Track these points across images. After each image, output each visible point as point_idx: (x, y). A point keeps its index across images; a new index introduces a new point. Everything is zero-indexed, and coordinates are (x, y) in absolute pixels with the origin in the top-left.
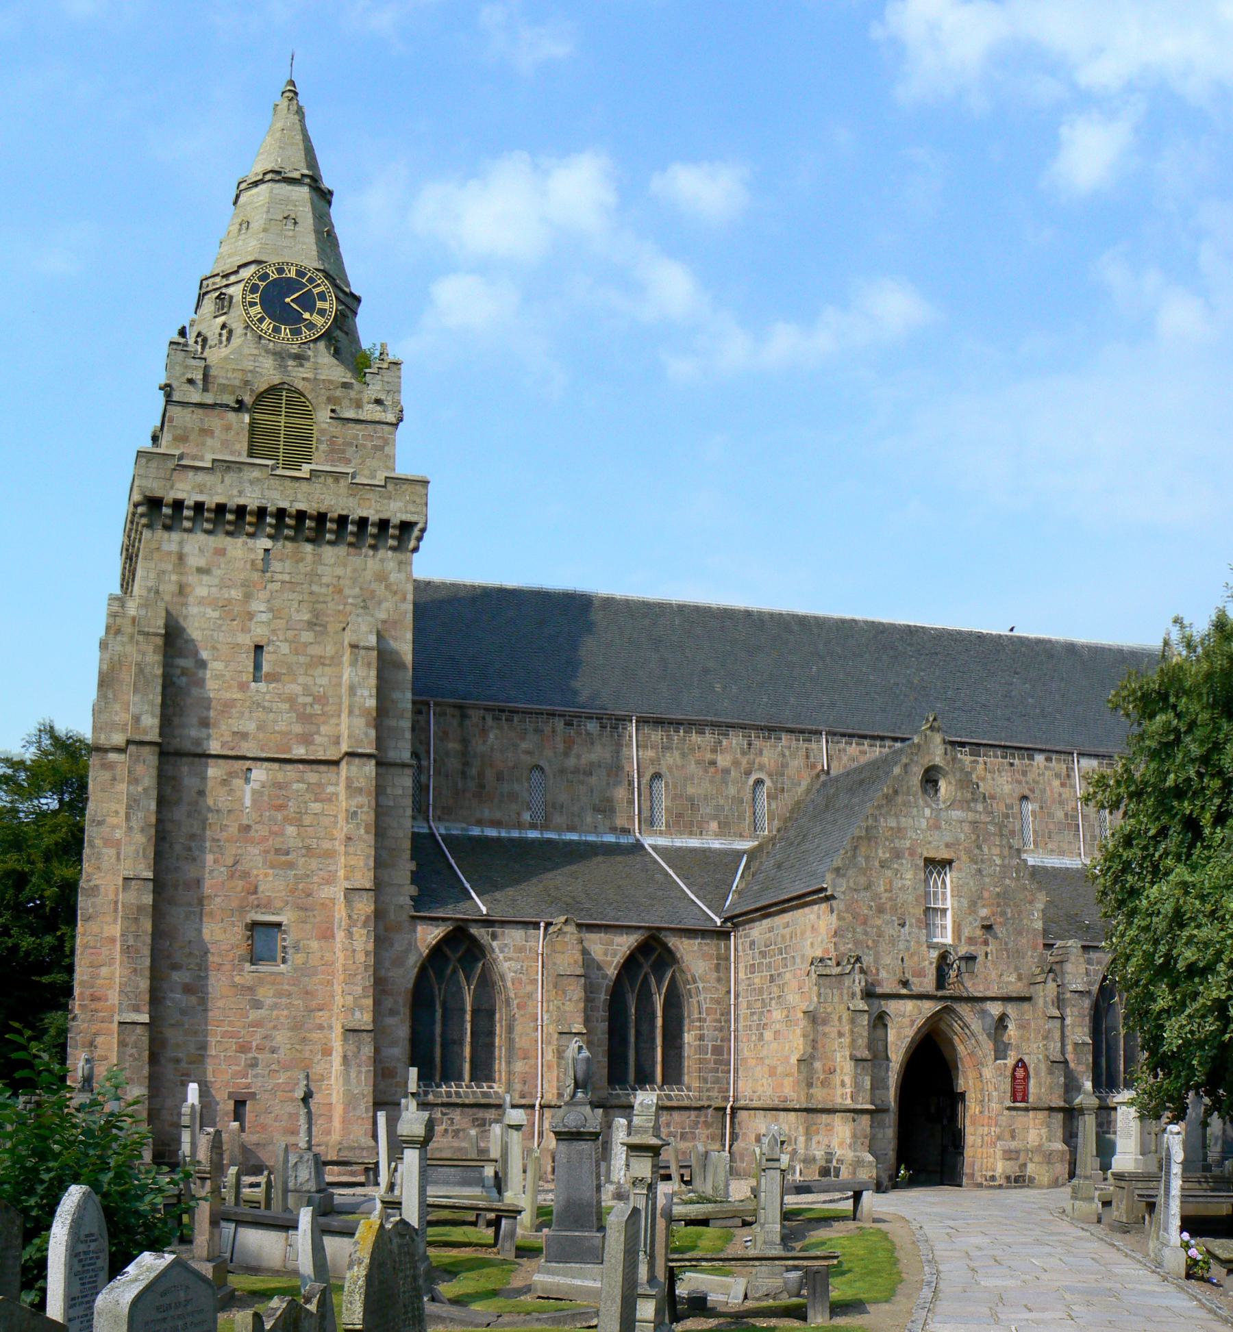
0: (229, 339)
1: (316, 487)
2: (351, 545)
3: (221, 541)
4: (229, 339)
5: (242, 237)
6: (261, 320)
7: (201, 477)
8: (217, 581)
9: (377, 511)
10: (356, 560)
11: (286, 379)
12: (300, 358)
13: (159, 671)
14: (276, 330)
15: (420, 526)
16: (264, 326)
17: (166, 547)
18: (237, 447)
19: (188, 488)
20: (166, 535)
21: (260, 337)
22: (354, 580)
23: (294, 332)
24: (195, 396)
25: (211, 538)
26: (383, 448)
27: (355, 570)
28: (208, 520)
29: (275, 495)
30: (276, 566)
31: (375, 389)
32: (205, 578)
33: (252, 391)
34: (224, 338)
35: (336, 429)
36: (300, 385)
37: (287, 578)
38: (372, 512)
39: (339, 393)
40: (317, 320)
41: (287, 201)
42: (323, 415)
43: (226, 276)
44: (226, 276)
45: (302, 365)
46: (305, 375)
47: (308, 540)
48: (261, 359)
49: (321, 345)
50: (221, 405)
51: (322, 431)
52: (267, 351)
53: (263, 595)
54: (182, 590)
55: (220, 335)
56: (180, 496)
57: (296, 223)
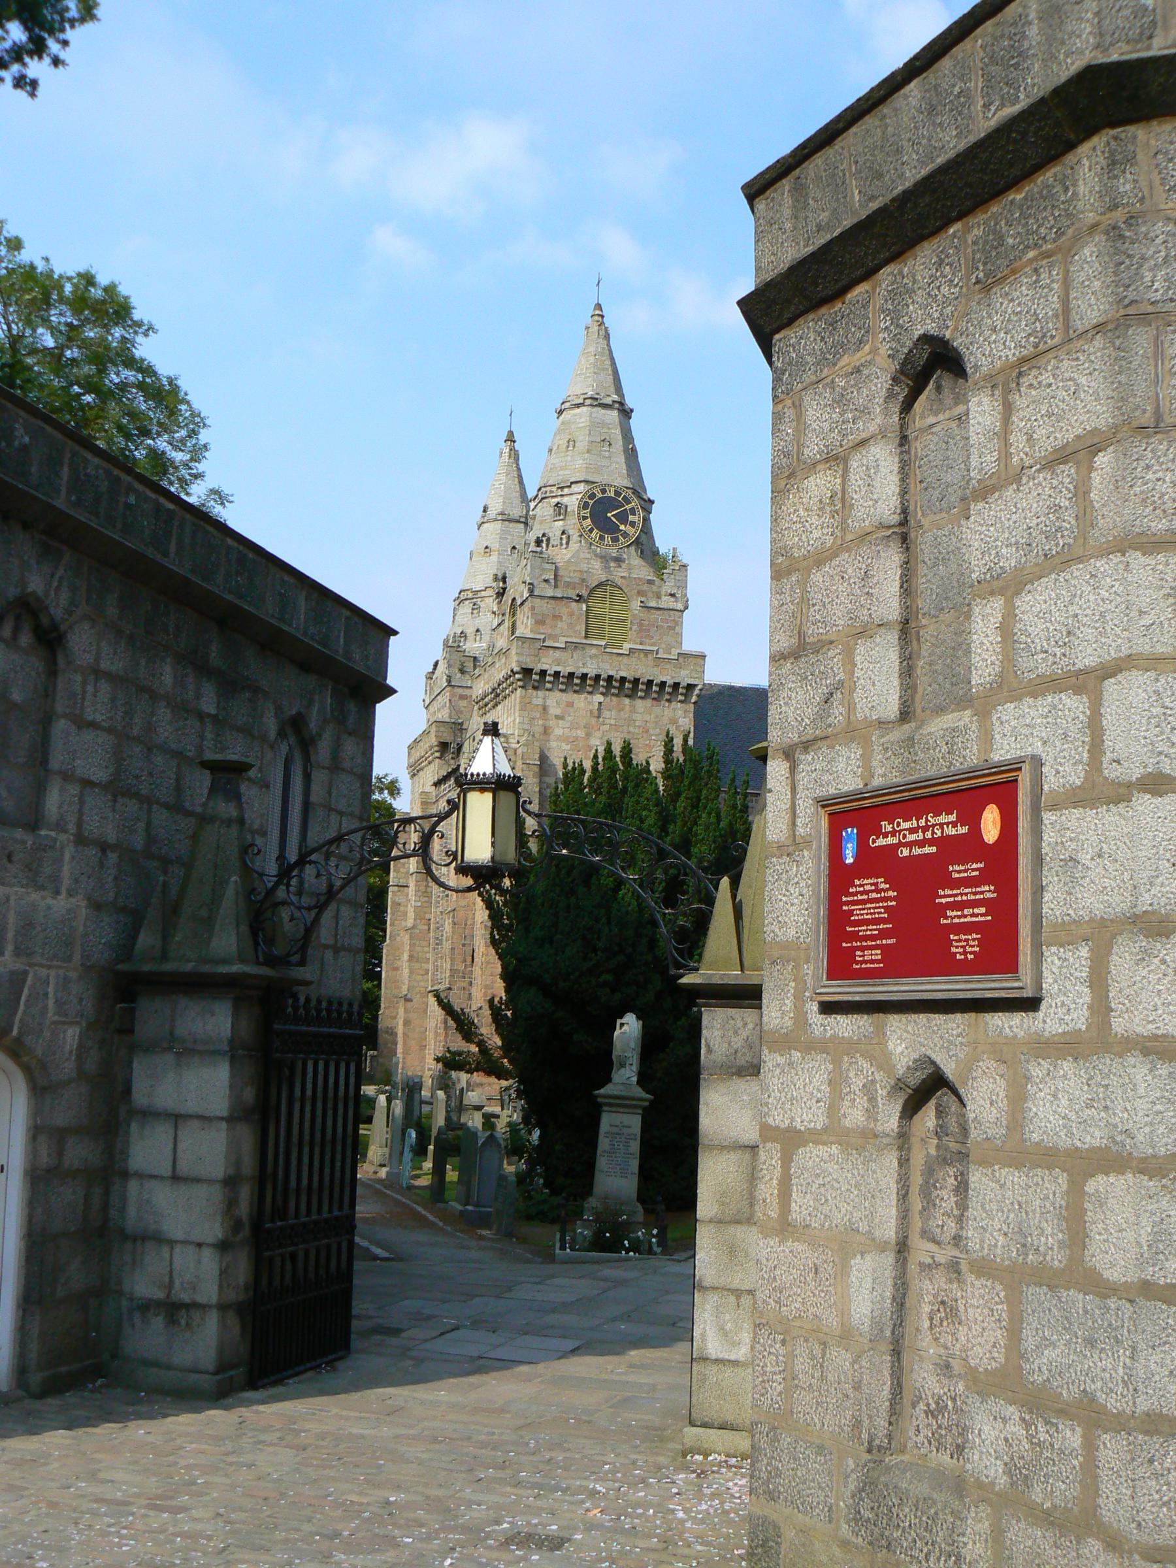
0: (567, 543)
1: (633, 660)
2: (654, 699)
3: (569, 696)
4: (567, 543)
5: (570, 453)
6: (591, 531)
7: (557, 654)
8: (568, 725)
9: (673, 678)
10: (657, 710)
11: (610, 577)
12: (618, 560)
13: (537, 789)
14: (602, 538)
15: (699, 687)
16: (593, 535)
17: (535, 701)
18: (578, 628)
19: (550, 662)
20: (535, 692)
21: (591, 544)
22: (656, 723)
23: (615, 540)
24: (550, 592)
25: (564, 695)
26: (675, 628)
27: (657, 716)
28: (562, 683)
29: (606, 666)
30: (606, 714)
31: (669, 586)
32: (561, 722)
33: (587, 586)
34: (564, 542)
35: (644, 615)
36: (619, 582)
37: (613, 722)
38: (669, 677)
39: (645, 587)
40: (630, 530)
41: (603, 424)
42: (636, 604)
43: (562, 488)
44: (562, 488)
45: (620, 567)
46: (623, 574)
47: (627, 696)
48: (592, 562)
49: (632, 549)
50: (567, 598)
51: (634, 616)
52: (596, 555)
53: (598, 734)
54: (546, 731)
55: (561, 539)
56: (545, 667)
57: (610, 445)
